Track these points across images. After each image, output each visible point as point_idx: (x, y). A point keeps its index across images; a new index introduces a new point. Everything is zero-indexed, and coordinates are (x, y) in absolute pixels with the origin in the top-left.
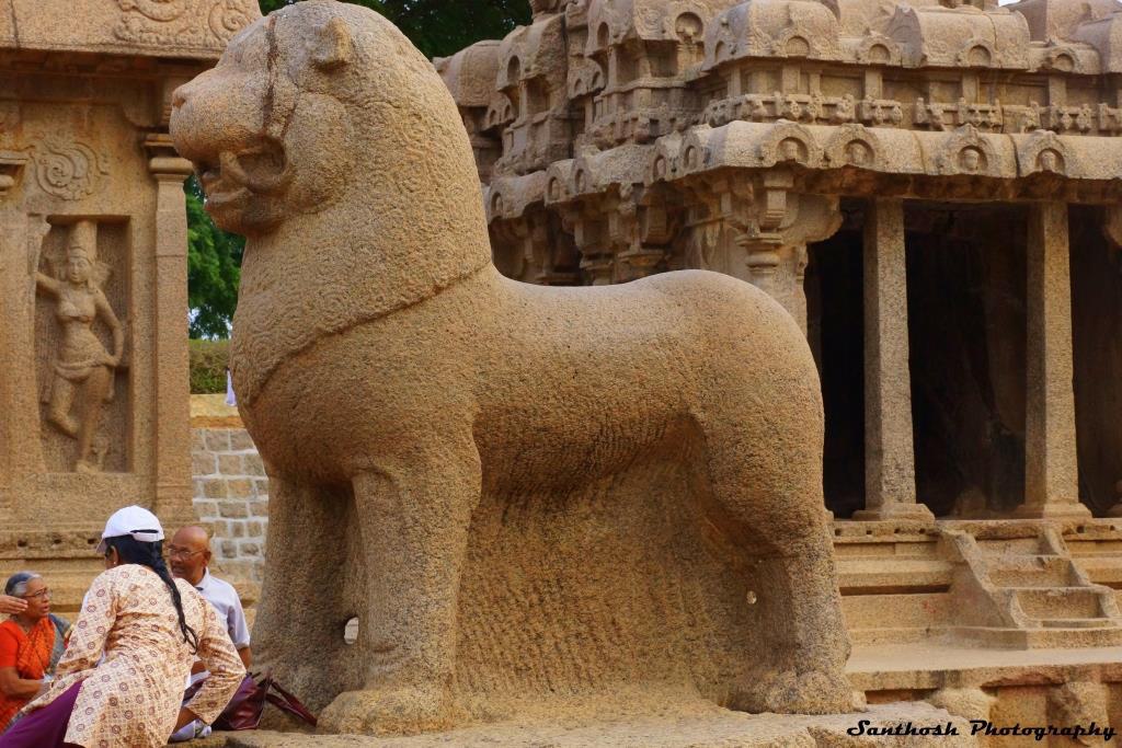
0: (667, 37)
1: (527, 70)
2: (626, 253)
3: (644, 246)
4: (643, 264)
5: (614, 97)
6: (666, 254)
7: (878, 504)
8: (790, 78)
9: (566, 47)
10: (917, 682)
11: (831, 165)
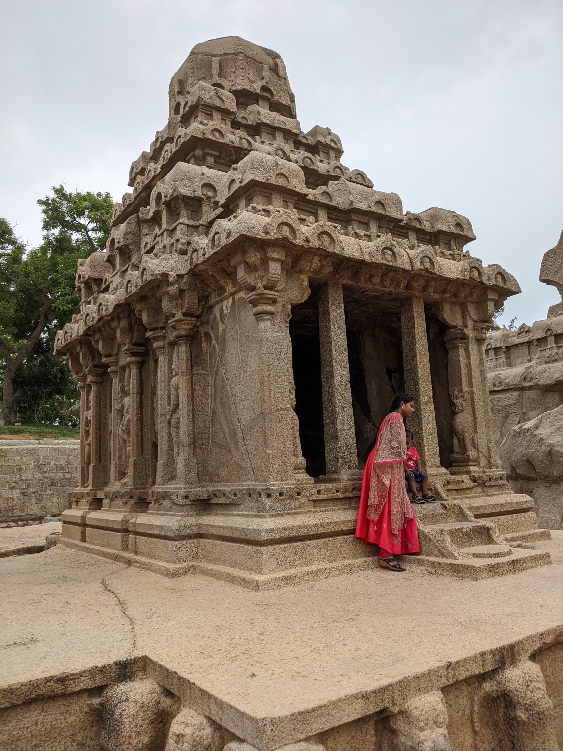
0: (196, 194)
1: (119, 242)
2: (174, 319)
3: (184, 315)
4: (184, 326)
5: (165, 234)
6: (198, 321)
8: (277, 201)
9: (140, 231)
10: (483, 665)
11: (311, 245)
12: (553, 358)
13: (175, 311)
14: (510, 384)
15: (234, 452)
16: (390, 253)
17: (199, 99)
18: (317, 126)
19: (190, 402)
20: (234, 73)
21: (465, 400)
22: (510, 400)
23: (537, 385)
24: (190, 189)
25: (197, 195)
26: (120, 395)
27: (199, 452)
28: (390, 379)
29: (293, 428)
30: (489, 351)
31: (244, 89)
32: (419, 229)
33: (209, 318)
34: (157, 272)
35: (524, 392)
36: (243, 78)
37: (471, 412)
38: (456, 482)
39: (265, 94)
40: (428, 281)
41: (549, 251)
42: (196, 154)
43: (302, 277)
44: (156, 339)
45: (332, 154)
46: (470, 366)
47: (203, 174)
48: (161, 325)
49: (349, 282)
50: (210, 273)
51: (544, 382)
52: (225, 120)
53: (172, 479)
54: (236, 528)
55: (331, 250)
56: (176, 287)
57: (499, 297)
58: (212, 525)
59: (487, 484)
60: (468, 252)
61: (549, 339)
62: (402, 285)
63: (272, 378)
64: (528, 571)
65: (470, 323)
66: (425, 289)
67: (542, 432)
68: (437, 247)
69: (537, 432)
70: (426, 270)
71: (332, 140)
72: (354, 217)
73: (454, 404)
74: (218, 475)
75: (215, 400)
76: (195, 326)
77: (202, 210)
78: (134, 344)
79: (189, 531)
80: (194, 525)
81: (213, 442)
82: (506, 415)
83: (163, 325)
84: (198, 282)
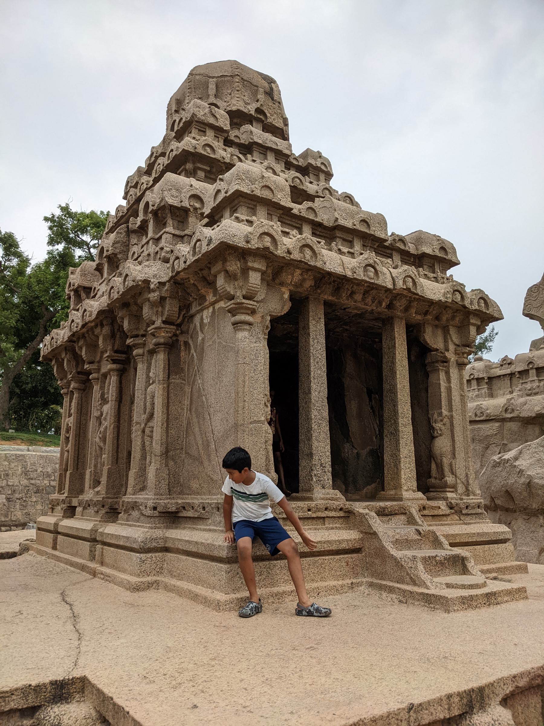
0: (183, 204)
1: (107, 251)
2: (153, 326)
3: (164, 322)
4: (163, 334)
5: (151, 242)
6: (177, 330)
7: (310, 490)
9: (129, 241)
10: (449, 709)
11: (292, 257)
12: (534, 391)
13: (154, 318)
14: (492, 414)
15: (206, 463)
16: (373, 270)
17: (194, 115)
18: (308, 149)
19: (165, 411)
20: (230, 94)
21: (444, 424)
22: (491, 431)
23: (518, 417)
24: (177, 199)
25: (184, 205)
26: (100, 402)
27: (171, 463)
28: (370, 400)
29: (266, 442)
30: (472, 381)
31: (238, 110)
32: (403, 250)
33: (189, 327)
34: (139, 278)
35: (505, 423)
36: (238, 99)
37: (450, 436)
38: (433, 508)
39: (259, 116)
40: (410, 302)
41: (532, 287)
42: (187, 167)
43: (283, 289)
44: (136, 346)
45: (322, 177)
46: (451, 391)
47: (191, 186)
48: (142, 332)
49: (330, 298)
50: (192, 282)
51: (524, 414)
52: (218, 137)
53: (143, 489)
54: (202, 543)
55: (312, 263)
56: (157, 294)
57: (481, 322)
58: (178, 539)
59: (464, 512)
60: (451, 276)
61: (530, 372)
62: (384, 304)
63: (246, 389)
64: (503, 606)
65: (452, 347)
66: (407, 309)
67: (522, 463)
68: (421, 269)
69: (517, 463)
70: (408, 289)
71: (322, 163)
72: (338, 234)
73: (433, 428)
74: (189, 488)
75: (190, 410)
76: (175, 335)
77: (188, 221)
78: (116, 352)
79: (154, 544)
80: (160, 538)
81: (186, 453)
82: (486, 445)
83: (144, 333)
84: (180, 290)
